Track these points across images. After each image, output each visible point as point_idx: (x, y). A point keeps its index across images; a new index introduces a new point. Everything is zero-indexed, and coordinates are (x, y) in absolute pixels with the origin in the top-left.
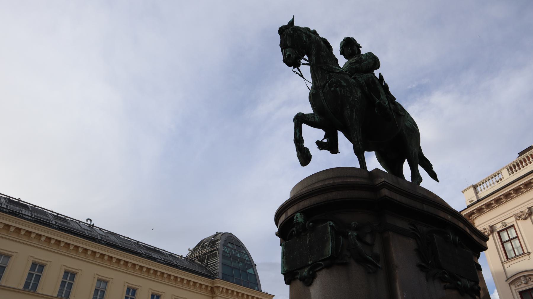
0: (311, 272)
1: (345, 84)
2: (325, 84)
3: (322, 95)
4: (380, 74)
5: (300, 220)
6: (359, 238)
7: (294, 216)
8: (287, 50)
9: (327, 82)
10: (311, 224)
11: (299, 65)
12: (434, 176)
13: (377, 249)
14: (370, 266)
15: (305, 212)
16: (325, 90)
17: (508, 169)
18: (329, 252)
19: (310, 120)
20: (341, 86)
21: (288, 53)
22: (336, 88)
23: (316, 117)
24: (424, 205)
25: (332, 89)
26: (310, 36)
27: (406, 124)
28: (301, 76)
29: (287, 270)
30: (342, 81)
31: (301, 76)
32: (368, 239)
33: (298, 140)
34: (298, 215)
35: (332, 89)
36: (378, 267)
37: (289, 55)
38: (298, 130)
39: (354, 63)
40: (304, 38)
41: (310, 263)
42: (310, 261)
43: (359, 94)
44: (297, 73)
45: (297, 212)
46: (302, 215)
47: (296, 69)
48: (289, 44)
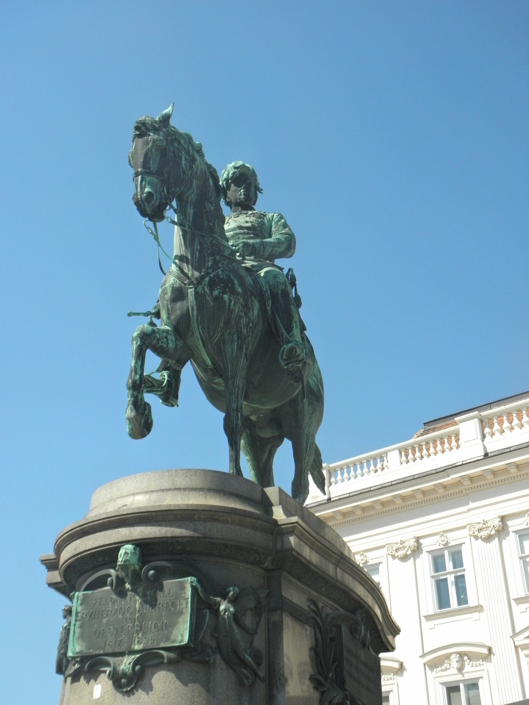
0: (137, 668)
1: (239, 290)
6: (236, 618)
7: (118, 549)
8: (148, 178)
9: (208, 274)
10: (152, 572)
11: (161, 217)
13: (259, 642)
14: (245, 671)
15: (143, 546)
16: (200, 289)
17: (400, 453)
18: (182, 636)
19: (160, 344)
20: (233, 292)
21: (147, 190)
22: (224, 293)
23: (169, 337)
24: (338, 570)
25: (216, 293)
27: (310, 380)
28: (156, 238)
29: (80, 652)
30: (236, 282)
32: (248, 621)
34: (129, 547)
35: (216, 293)
36: (256, 675)
38: (139, 363)
39: (247, 228)
40: (183, 163)
41: (137, 647)
42: (139, 643)
43: (256, 312)
45: (127, 542)
46: (138, 552)
47: (150, 224)
48: (153, 167)
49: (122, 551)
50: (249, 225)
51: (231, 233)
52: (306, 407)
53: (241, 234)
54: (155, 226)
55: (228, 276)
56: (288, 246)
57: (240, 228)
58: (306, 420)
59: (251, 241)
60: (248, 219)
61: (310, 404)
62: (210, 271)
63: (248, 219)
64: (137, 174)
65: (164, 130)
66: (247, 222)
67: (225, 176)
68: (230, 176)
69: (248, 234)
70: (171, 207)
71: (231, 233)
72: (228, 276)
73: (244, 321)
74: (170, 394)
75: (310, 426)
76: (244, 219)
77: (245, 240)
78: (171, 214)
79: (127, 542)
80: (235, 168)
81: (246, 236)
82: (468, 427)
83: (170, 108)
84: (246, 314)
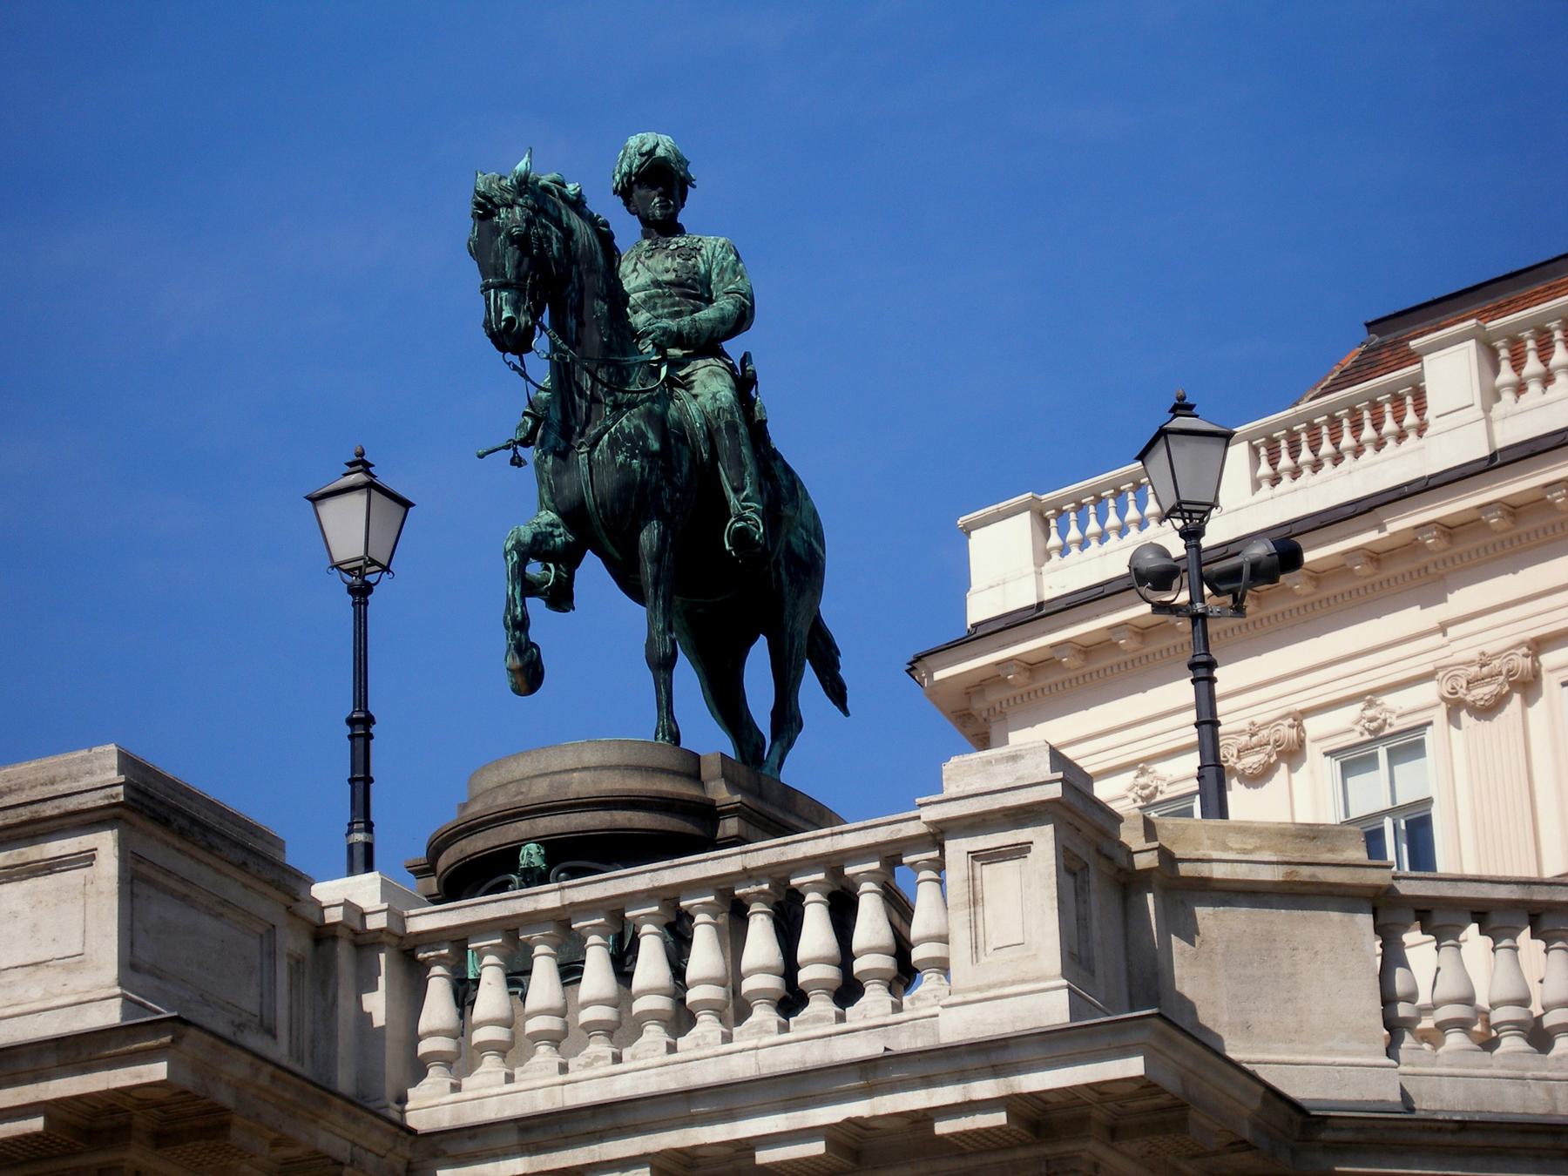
2: (599, 437)
3: (585, 470)
4: (746, 358)
5: (537, 861)
7: (518, 849)
8: (504, 294)
11: (529, 349)
12: (837, 692)
21: (505, 315)
22: (633, 456)
23: (557, 532)
25: (620, 458)
26: (568, 233)
27: (793, 540)
28: (524, 374)
30: (651, 435)
31: (524, 374)
33: (520, 625)
34: (532, 847)
35: (620, 458)
37: (510, 321)
39: (670, 284)
40: (555, 247)
44: (515, 368)
47: (515, 359)
48: (510, 273)
49: (524, 851)
50: (671, 276)
51: (642, 294)
52: (786, 590)
53: (659, 296)
54: (521, 359)
55: (637, 428)
56: (742, 319)
57: (657, 284)
58: (788, 610)
59: (672, 324)
60: (668, 263)
61: (791, 583)
62: (609, 423)
63: (668, 263)
64: (486, 288)
65: (521, 201)
66: (667, 271)
67: (625, 168)
68: (634, 170)
69: (671, 296)
70: (543, 328)
71: (642, 294)
72: (637, 428)
73: (666, 494)
74: (561, 597)
75: (794, 619)
76: (664, 266)
77: (665, 323)
78: (541, 342)
79: (529, 840)
80: (642, 155)
81: (668, 301)
82: (1449, 368)
83: (526, 159)
84: (670, 482)
